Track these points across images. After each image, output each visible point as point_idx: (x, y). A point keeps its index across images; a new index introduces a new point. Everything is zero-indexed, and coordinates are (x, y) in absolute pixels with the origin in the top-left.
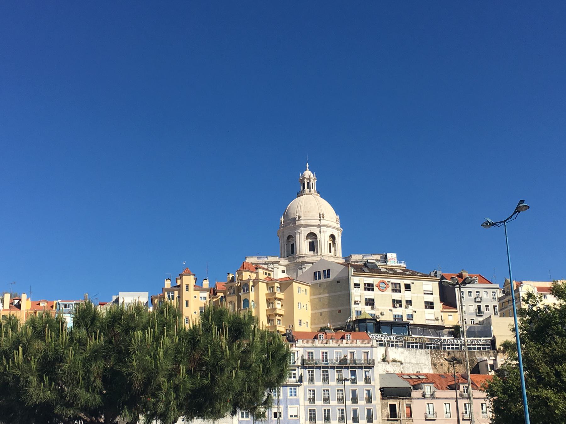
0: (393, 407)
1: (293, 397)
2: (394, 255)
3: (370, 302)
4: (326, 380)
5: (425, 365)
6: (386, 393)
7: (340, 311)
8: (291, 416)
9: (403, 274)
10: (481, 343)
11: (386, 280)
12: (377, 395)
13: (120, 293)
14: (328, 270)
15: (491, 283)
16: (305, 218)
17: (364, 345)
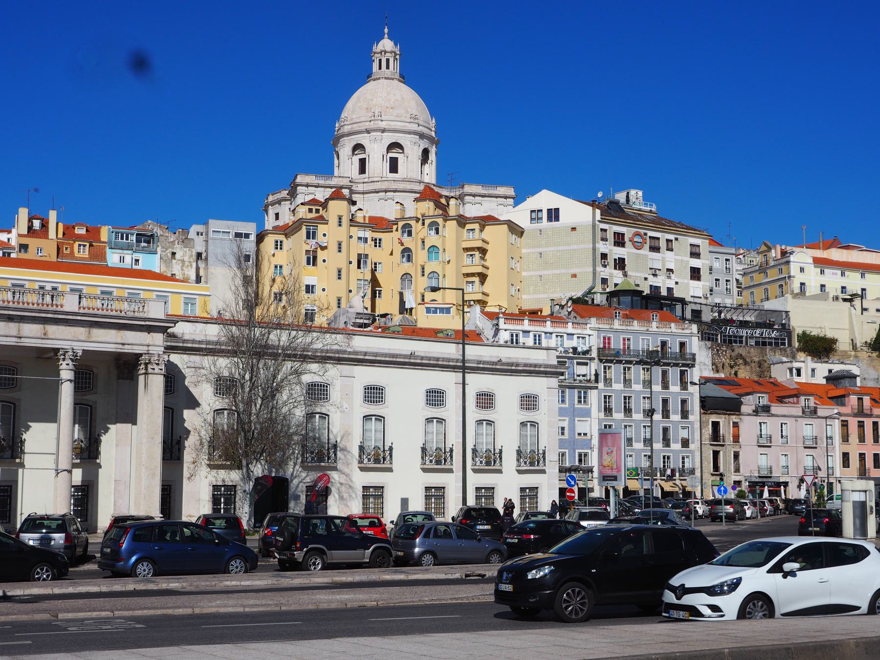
0: (716, 425)
1: (582, 406)
2: (640, 193)
3: (620, 264)
4: (627, 382)
5: (705, 364)
6: (708, 405)
7: (574, 276)
8: (580, 434)
9: (659, 222)
10: (773, 335)
11: (642, 231)
12: (695, 405)
13: (211, 221)
14: (557, 210)
15: (721, 245)
16: (387, 118)
17: (681, 331)
